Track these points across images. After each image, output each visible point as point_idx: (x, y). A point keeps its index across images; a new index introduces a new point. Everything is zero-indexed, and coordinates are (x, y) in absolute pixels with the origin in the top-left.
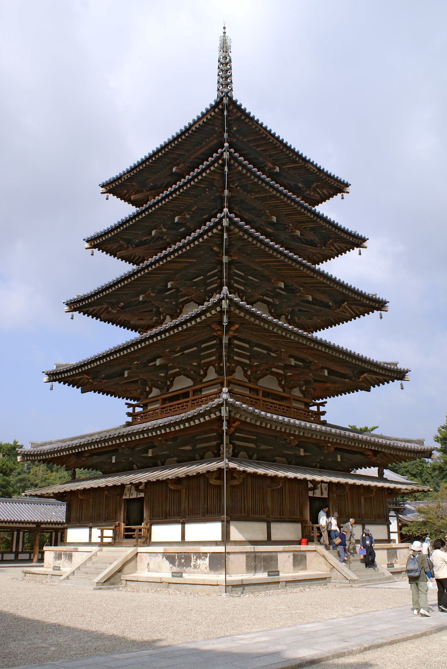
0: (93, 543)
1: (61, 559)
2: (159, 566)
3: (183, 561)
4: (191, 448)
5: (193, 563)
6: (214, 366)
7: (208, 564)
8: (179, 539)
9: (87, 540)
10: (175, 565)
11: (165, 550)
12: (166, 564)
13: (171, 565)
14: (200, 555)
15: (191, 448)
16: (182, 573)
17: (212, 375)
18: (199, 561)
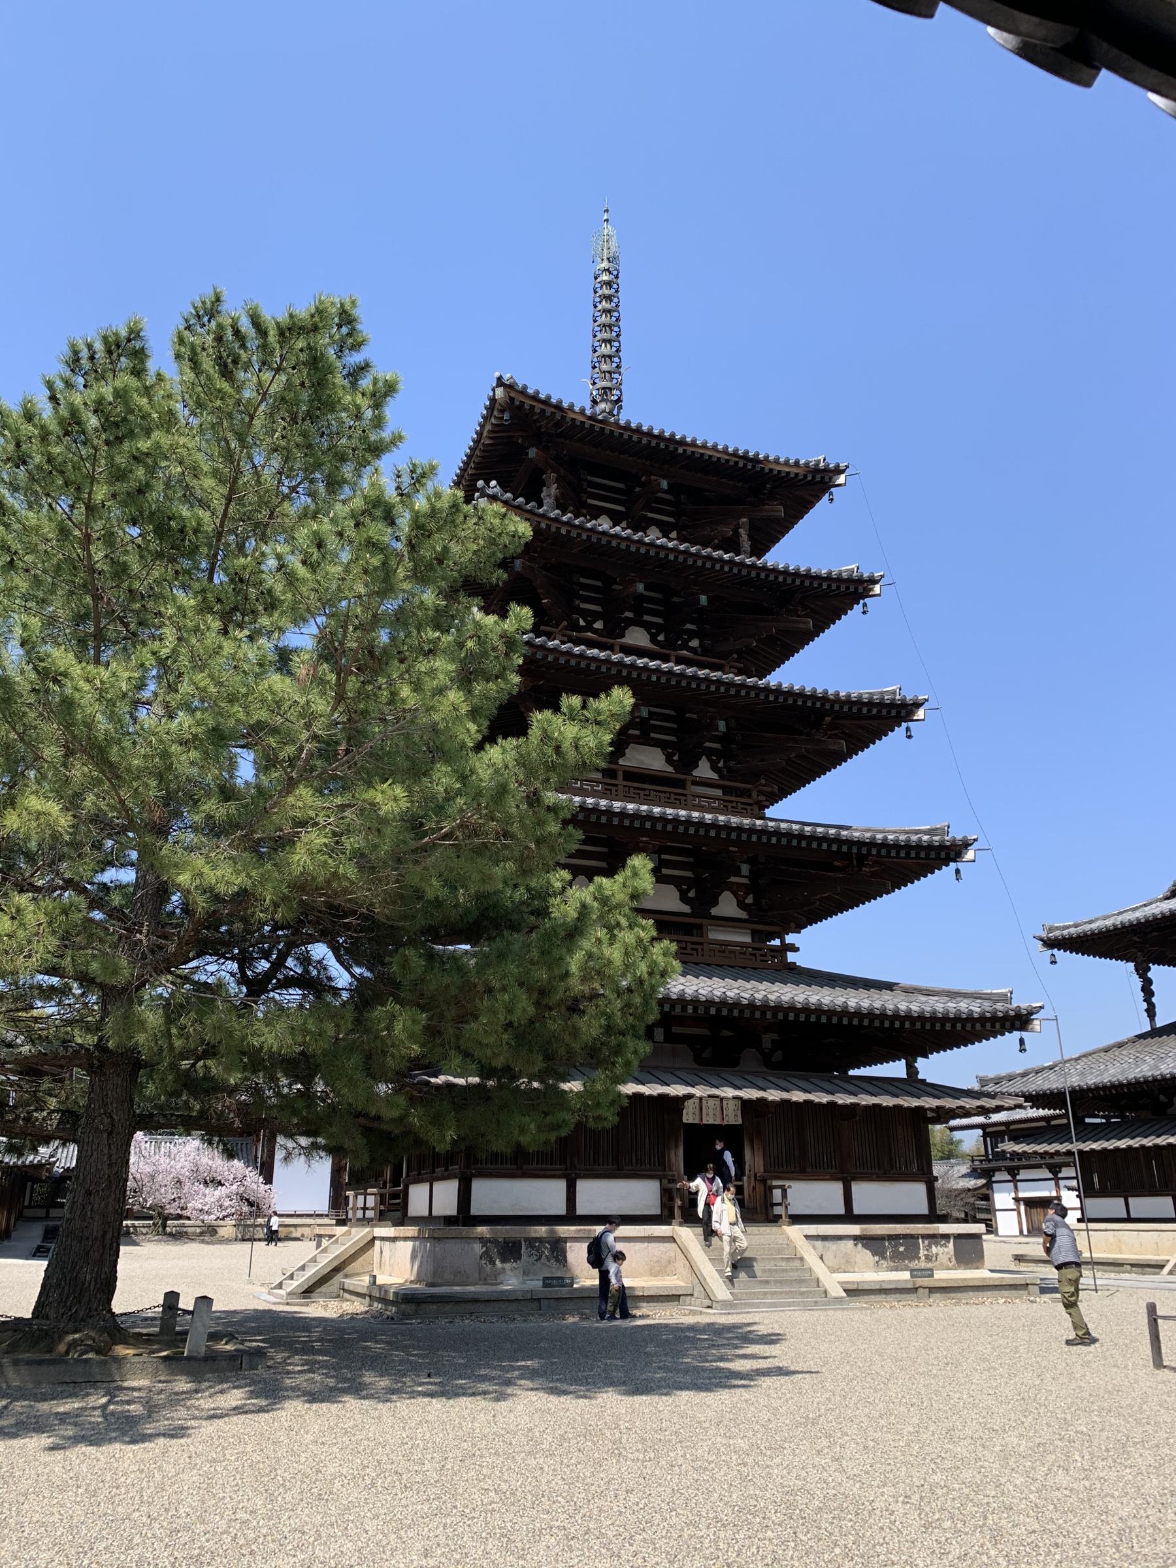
0: (475, 1217)
1: (520, 1258)
2: (848, 1261)
3: (902, 1249)
4: (709, 1033)
5: (922, 1253)
6: (736, 895)
7: (952, 1253)
8: (842, 1211)
9: (560, 1209)
10: (884, 1258)
11: (862, 1230)
12: (864, 1256)
13: (877, 1258)
14: (933, 1238)
15: (709, 1033)
16: (931, 1270)
17: (727, 906)
18: (934, 1249)
